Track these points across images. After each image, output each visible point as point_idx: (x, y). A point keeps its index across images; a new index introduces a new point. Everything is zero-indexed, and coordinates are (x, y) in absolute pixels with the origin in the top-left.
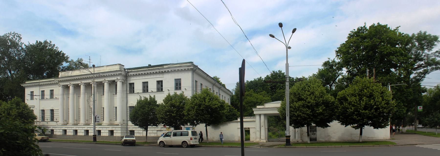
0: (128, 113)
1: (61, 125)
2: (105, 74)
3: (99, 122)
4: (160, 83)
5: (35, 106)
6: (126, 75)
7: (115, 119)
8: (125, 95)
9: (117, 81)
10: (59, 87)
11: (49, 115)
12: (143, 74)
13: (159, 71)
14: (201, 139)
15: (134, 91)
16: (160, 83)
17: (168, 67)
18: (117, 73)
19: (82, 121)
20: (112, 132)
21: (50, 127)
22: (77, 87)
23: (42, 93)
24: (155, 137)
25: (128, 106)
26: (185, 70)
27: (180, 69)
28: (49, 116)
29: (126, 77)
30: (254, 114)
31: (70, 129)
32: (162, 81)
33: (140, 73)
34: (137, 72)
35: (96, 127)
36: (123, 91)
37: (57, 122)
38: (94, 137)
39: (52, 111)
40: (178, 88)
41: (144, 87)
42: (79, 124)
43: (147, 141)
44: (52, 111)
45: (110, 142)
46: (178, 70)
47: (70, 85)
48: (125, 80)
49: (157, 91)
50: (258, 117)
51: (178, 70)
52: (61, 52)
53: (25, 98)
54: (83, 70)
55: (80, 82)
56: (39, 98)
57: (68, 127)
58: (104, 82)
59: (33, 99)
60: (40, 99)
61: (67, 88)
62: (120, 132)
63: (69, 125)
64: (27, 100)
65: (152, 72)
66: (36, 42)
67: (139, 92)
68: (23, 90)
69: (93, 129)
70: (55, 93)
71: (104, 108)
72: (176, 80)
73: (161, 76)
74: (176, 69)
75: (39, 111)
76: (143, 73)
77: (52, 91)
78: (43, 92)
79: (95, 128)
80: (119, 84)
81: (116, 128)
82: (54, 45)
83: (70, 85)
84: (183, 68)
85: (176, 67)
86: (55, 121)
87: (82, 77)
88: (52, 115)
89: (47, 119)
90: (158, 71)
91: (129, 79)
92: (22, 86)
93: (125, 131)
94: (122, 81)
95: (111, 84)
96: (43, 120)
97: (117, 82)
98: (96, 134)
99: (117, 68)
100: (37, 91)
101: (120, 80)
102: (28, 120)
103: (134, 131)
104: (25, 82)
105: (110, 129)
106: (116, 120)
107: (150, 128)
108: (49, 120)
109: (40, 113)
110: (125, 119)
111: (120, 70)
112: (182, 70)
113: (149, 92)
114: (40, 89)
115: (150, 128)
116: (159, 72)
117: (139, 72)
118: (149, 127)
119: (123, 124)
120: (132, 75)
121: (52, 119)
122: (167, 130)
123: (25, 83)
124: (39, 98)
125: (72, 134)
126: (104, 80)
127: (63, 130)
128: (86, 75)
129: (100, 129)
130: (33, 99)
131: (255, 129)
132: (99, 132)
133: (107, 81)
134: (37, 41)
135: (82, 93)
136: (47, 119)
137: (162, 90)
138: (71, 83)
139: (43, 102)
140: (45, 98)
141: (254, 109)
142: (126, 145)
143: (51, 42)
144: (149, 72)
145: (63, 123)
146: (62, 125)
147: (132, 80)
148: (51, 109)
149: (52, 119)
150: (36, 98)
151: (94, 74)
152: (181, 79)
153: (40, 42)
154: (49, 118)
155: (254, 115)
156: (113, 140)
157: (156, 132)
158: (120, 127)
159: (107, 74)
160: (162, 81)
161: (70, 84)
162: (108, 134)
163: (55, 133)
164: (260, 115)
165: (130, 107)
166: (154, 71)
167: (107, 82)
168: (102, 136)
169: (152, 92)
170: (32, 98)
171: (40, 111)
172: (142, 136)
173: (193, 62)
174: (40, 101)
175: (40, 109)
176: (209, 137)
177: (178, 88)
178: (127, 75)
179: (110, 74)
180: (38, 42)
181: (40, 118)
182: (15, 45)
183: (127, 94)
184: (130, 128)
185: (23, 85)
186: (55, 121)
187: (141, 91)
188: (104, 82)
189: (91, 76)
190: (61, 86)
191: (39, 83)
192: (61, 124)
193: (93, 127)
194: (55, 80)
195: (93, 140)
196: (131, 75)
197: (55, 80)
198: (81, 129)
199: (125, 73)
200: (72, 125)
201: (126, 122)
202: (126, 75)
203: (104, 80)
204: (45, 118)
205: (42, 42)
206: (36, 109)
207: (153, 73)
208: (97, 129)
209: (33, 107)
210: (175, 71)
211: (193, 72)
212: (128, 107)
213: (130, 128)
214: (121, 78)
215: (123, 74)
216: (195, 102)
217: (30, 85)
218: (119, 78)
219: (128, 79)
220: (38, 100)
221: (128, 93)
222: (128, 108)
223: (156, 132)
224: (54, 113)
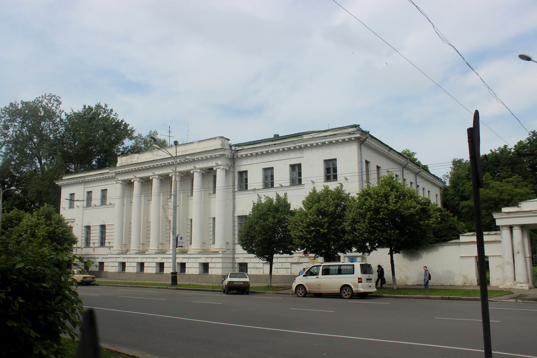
0: (236, 228)
1: (116, 253)
2: (195, 157)
3: (182, 247)
4: (296, 169)
5: (75, 219)
6: (233, 156)
7: (211, 242)
8: (231, 194)
9: (216, 169)
10: (116, 183)
11: (98, 235)
12: (264, 152)
13: (294, 145)
14: (380, 280)
15: (246, 186)
16: (296, 169)
17: (311, 137)
18: (217, 154)
19: (153, 246)
20: (205, 267)
21: (99, 258)
22: (147, 182)
23: (88, 196)
24: (287, 276)
25: (236, 215)
26: (344, 141)
27: (333, 139)
28: (98, 238)
29: (234, 160)
30: (497, 224)
31: (132, 260)
32: (299, 165)
33: (259, 151)
34: (252, 151)
35: (177, 256)
36: (226, 187)
37: (110, 248)
38: (172, 277)
39: (103, 227)
40: (332, 177)
41: (265, 178)
42: (147, 251)
43: (273, 285)
45: (202, 285)
46: (331, 143)
47: (135, 179)
48: (232, 166)
49: (291, 185)
50: (505, 233)
51: (331, 143)
52: (122, 121)
53: (61, 205)
54: (158, 150)
55: (152, 174)
56: (83, 205)
57: (128, 258)
58: (194, 172)
59: (73, 207)
60: (85, 206)
61: (129, 184)
62: (220, 265)
63: (130, 253)
64: (63, 208)
65: (280, 148)
66: (83, 107)
67: (257, 188)
68: (58, 191)
69: (171, 260)
70: (109, 194)
71: (191, 220)
72: (326, 161)
73: (298, 154)
74: (327, 140)
75: (82, 228)
76: (264, 150)
77: (104, 191)
78: (90, 193)
79: (175, 259)
81: (213, 259)
82: (112, 110)
83: (135, 179)
84: (340, 138)
85: (326, 136)
86: (106, 247)
87: (155, 164)
88: (102, 235)
89: (94, 243)
90: (292, 146)
91: (238, 163)
93: (230, 265)
95: (204, 175)
96: (87, 245)
97: (216, 171)
98: (176, 271)
99: (217, 144)
100: (80, 192)
102: (64, 245)
103: (246, 264)
104: (62, 177)
105: (203, 261)
106: (214, 243)
107: (277, 258)
108: (97, 245)
109: (83, 232)
110: (231, 241)
111: (222, 147)
112: (337, 142)
113: (275, 186)
115: (277, 258)
116: (295, 148)
117: (256, 150)
118: (275, 255)
119: (226, 250)
120: (244, 156)
121: (102, 243)
122: (311, 261)
123: (62, 179)
124: (83, 205)
125: (135, 272)
126: (194, 168)
127: (120, 263)
128: (162, 160)
129: (184, 261)
130: (73, 207)
131: (499, 258)
132: (183, 266)
133: (199, 168)
134: (85, 106)
135: (156, 194)
136: (94, 243)
137: (300, 181)
138: (136, 175)
139: (89, 212)
140: (92, 205)
141: (495, 216)
142: (231, 292)
143: (106, 106)
144: (275, 148)
145: (121, 249)
146: (118, 254)
147: (243, 165)
148: (102, 224)
149: (102, 243)
150: (78, 205)
151: (176, 157)
152: (335, 160)
153: (89, 106)
154: (98, 241)
155: (497, 228)
156: (208, 283)
157: (288, 265)
158: (221, 256)
159: (199, 157)
160: (299, 165)
161: (134, 177)
162: (198, 270)
163: (105, 269)
164: (511, 228)
165: (240, 217)
166: (285, 147)
167: (199, 171)
168: (187, 274)
169: (282, 186)
170: (71, 206)
171: (84, 229)
172: (262, 274)
173: (359, 126)
176: (397, 277)
177: (332, 177)
178: (235, 157)
179: (204, 156)
180: (87, 107)
181: (83, 241)
182: (50, 115)
184: (238, 258)
186: (106, 247)
187: (260, 186)
188: (194, 172)
189: (170, 161)
190: (119, 183)
191: (84, 178)
192: (116, 252)
193: (171, 256)
194: (110, 172)
195: (171, 282)
196: (242, 156)
197: (110, 172)
198: (151, 260)
199: (231, 153)
200: (136, 253)
201: (231, 247)
202: (233, 156)
203: (194, 168)
204: (91, 241)
205: (92, 107)
206: (77, 224)
207: (284, 149)
208: (179, 260)
209: (72, 222)
210: (324, 144)
211: (361, 145)
212: (236, 217)
213: (238, 258)
214: (225, 163)
215: (228, 155)
216: (367, 203)
217: (69, 182)
218: (220, 162)
219: (236, 164)
220: (81, 208)
221: (236, 190)
222: (236, 220)
223: (288, 265)
224: (107, 231)
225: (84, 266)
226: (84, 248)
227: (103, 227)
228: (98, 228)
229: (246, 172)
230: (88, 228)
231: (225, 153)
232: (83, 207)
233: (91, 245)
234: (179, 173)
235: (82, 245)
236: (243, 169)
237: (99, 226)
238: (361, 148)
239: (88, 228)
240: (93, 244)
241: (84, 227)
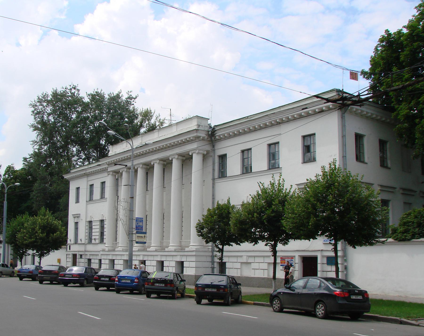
5: (80, 214)
28: (98, 234)
44: (102, 221)
68: (67, 183)
78: (92, 186)
80: (197, 160)
89: (95, 239)
92: (66, 179)
94: (201, 152)
96: (90, 242)
101: (197, 151)
108: (97, 241)
109: (87, 228)
114: (88, 181)
136: (95, 239)
149: (102, 240)
174: (87, 204)
175: (86, 218)
183: (214, 179)
185: (66, 177)
204: (93, 237)
205: (88, 102)
225: (88, 263)
226: (87, 244)
227: (102, 221)
228: (98, 223)
229: (225, 155)
230: (90, 222)
231: (199, 134)
232: (86, 201)
233: (93, 241)
234: (160, 161)
235: (85, 242)
236: (221, 152)
237: (99, 221)
238: (343, 117)
239: (90, 222)
240: (94, 240)
241: (87, 222)
